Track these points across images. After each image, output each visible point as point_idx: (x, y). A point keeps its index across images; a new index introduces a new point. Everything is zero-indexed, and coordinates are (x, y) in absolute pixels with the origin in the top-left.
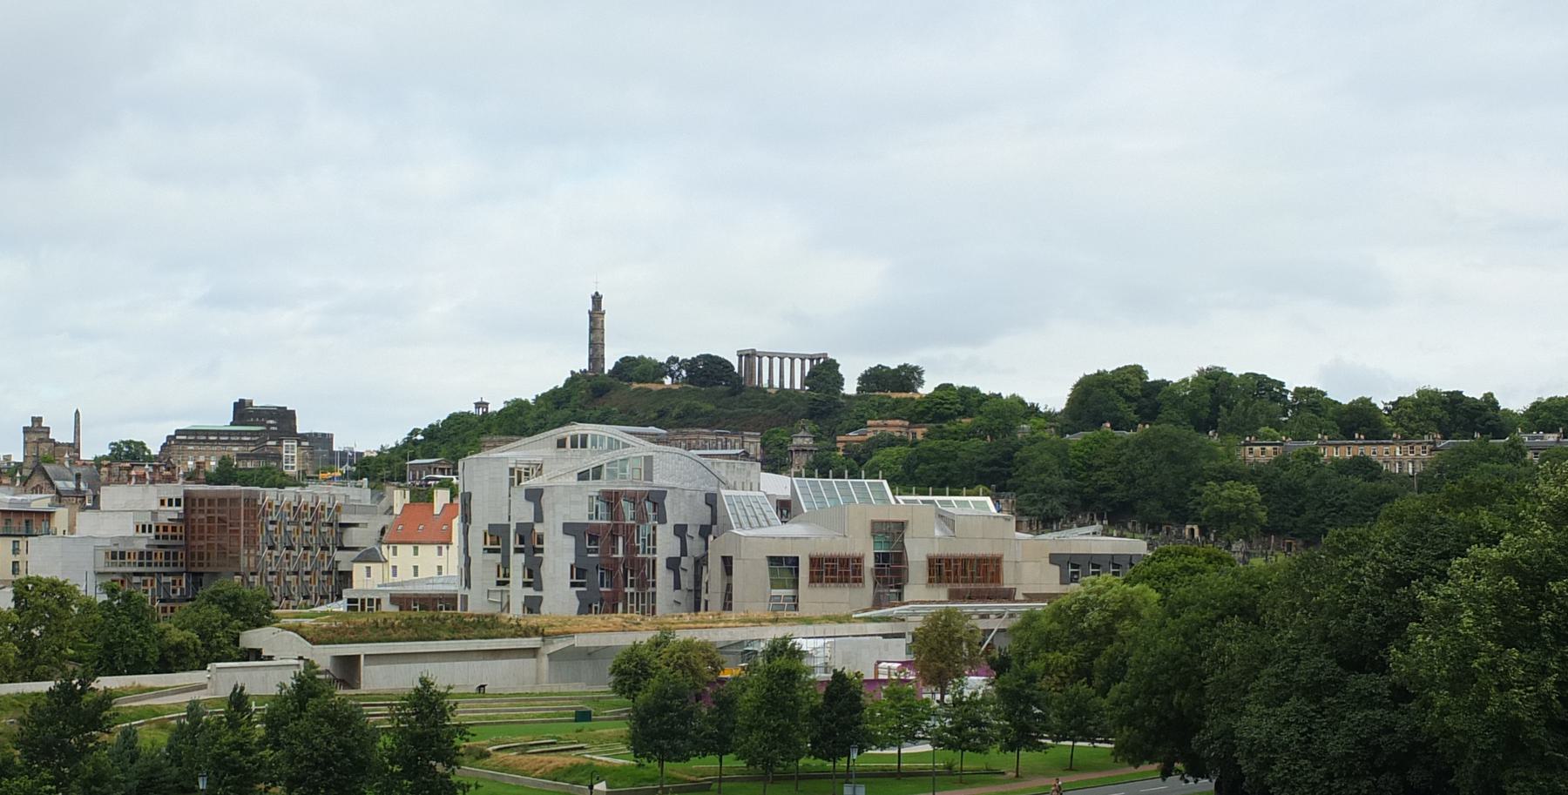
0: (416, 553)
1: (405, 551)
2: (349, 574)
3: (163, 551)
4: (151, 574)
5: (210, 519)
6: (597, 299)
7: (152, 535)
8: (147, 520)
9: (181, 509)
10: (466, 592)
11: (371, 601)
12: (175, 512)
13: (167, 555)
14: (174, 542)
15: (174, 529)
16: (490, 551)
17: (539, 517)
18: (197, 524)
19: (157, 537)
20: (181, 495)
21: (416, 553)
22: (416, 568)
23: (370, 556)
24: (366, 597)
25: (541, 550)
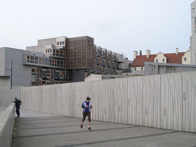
3: (57, 60)
4: (51, 68)
6: (141, 51)
7: (52, 53)
9: (64, 45)
13: (58, 62)
14: (61, 57)
15: (61, 52)
19: (54, 54)
20: (64, 40)
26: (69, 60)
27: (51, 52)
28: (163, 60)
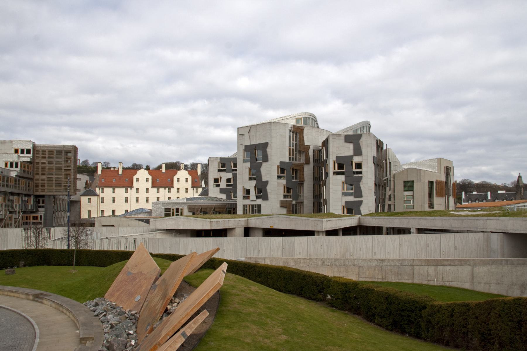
0: (114, 192)
1: (108, 191)
2: (79, 202)
5: (50, 163)
7: (18, 169)
8: (14, 158)
9: (30, 156)
10: (259, 201)
11: (177, 210)
12: (27, 157)
15: (28, 167)
16: (279, 177)
17: (358, 151)
18: (40, 166)
20: (30, 147)
21: (114, 192)
22: (114, 199)
23: (90, 192)
24: (177, 207)
25: (361, 173)
26: (38, 179)
27: (17, 166)
28: (147, 180)
